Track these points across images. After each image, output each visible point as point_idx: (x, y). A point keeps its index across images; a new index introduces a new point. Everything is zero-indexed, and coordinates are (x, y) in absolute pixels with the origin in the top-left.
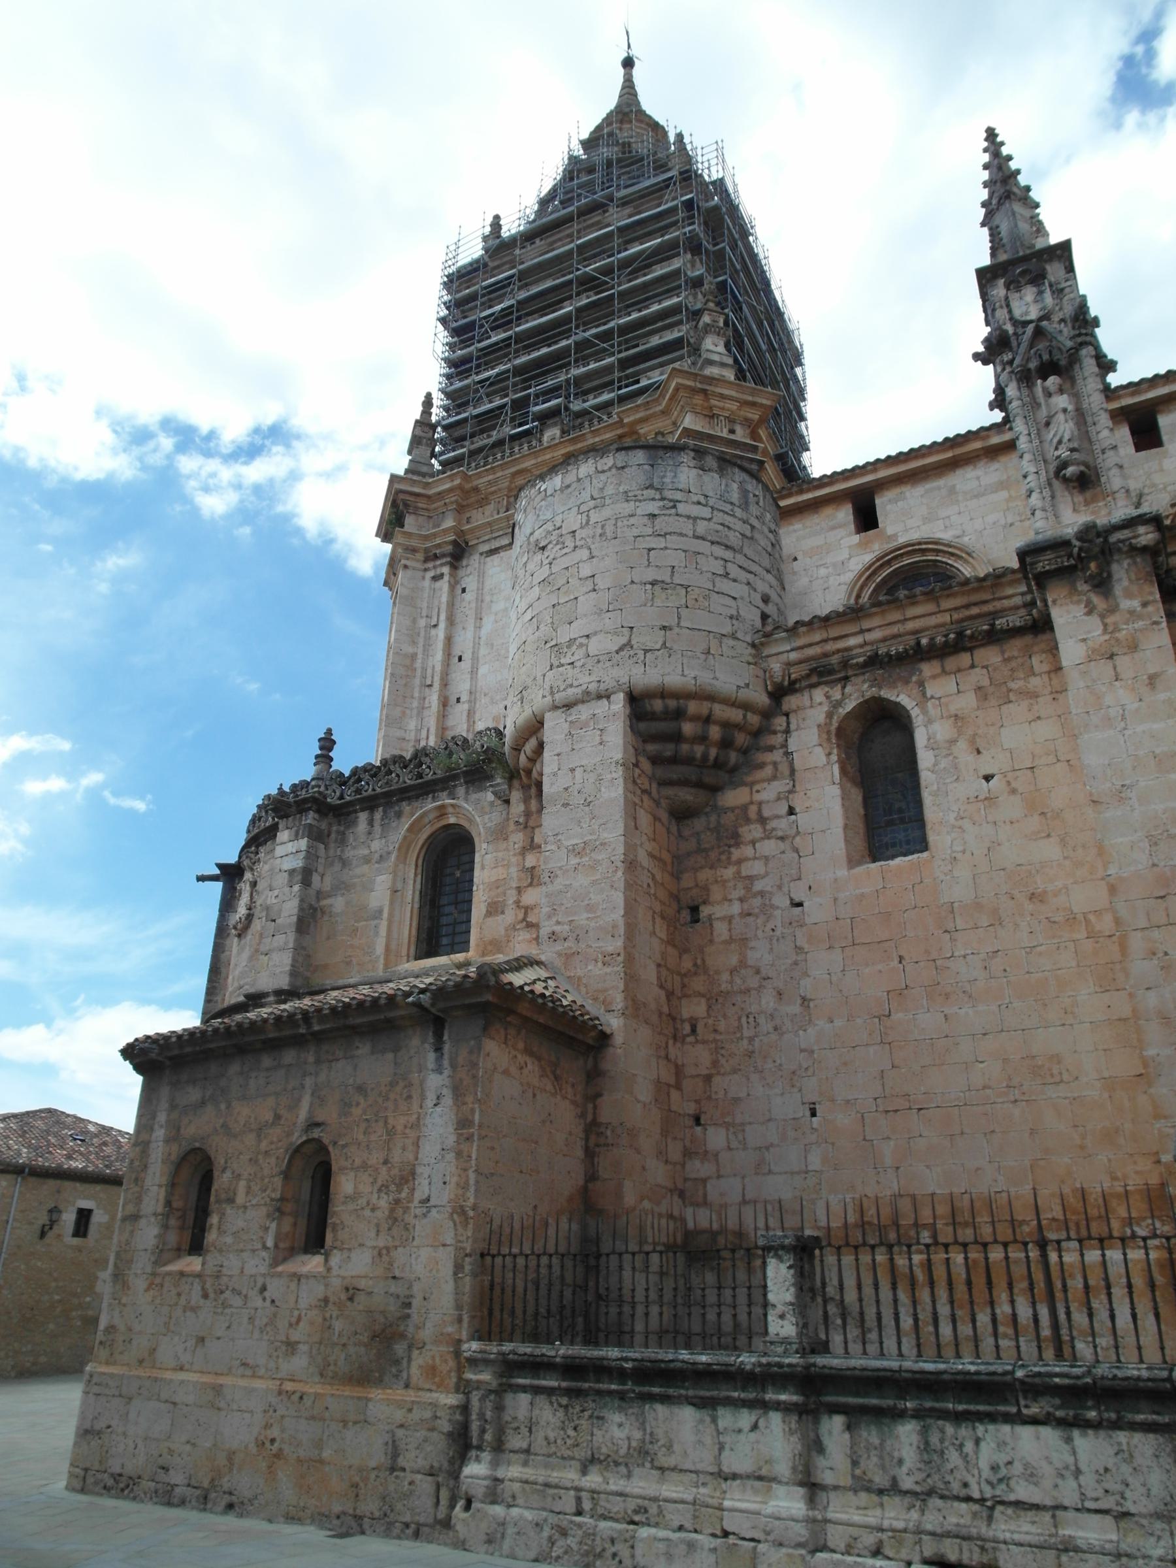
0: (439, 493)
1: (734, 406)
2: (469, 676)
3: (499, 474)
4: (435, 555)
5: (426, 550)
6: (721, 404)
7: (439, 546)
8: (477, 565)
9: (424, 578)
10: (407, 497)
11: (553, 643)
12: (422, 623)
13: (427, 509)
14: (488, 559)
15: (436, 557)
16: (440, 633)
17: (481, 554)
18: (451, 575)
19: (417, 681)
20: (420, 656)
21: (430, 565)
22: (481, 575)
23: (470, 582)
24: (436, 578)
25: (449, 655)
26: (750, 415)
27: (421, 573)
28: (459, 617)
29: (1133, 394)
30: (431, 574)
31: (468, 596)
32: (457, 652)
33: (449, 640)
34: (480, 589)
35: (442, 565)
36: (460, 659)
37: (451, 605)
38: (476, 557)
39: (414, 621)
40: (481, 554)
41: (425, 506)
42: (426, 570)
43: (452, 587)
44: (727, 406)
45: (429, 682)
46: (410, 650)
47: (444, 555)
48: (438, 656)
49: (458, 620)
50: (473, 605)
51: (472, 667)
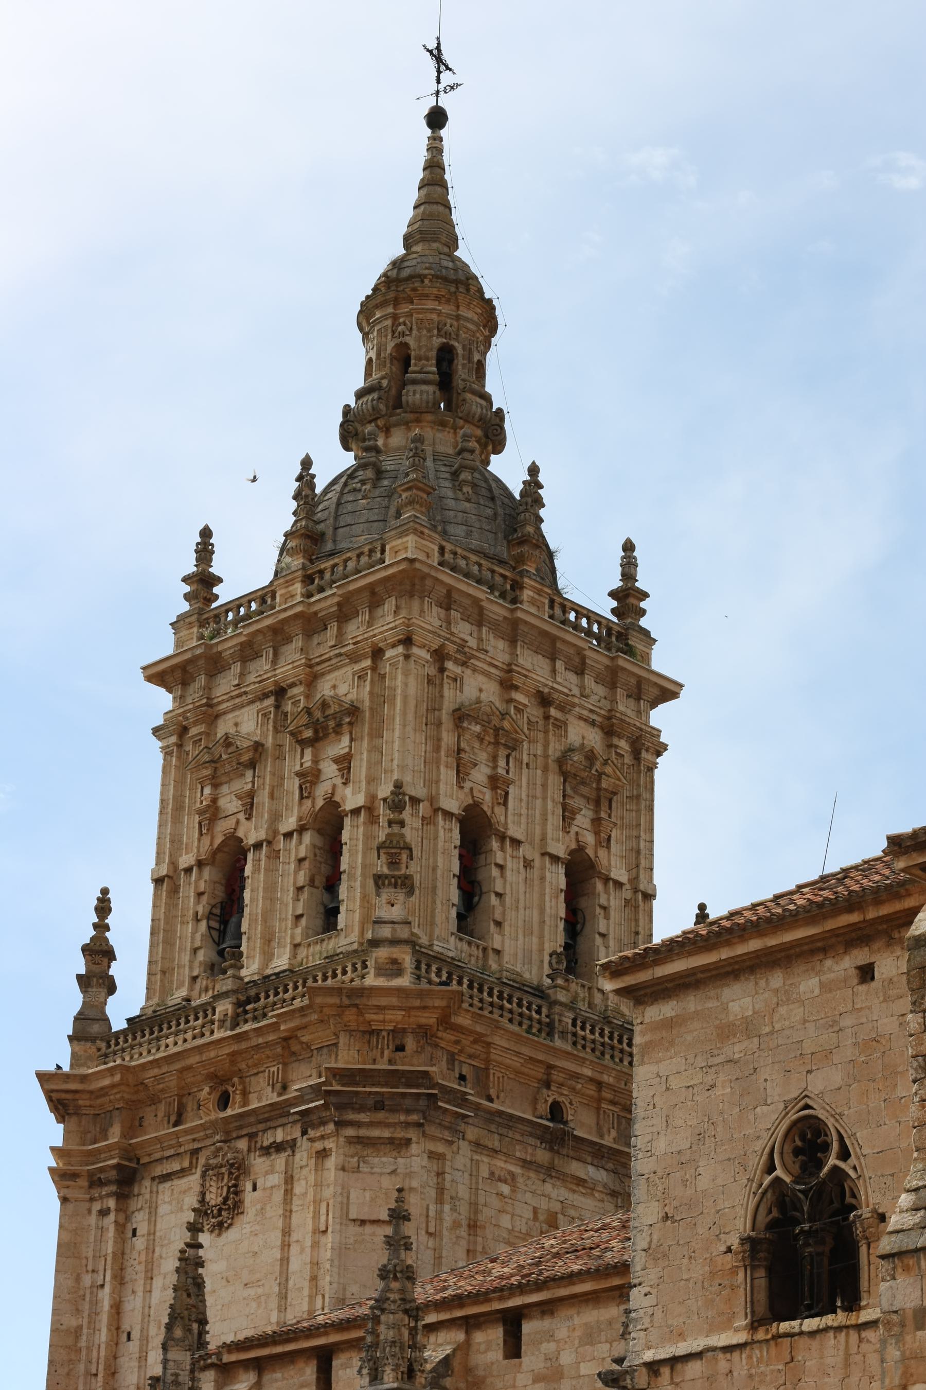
0: (102, 1089)
1: (398, 1015)
2: (136, 1364)
3: (165, 1069)
4: (100, 1179)
5: (91, 1174)
6: (381, 1017)
7: (101, 1170)
8: (147, 1196)
9: (90, 1211)
10: (64, 1096)
11: (251, 1292)
12: (87, 1280)
13: (90, 1106)
14: (161, 1187)
15: (101, 1183)
16: (105, 1297)
17: (153, 1179)
18: (118, 1210)
19: (81, 1367)
20: (85, 1331)
21: (96, 1193)
22: (153, 1211)
23: (140, 1221)
24: (104, 1213)
25: (118, 1329)
26: (423, 1021)
27: (87, 1205)
28: (129, 1274)
29: (501, 1299)
30: (97, 1206)
31: (139, 1243)
32: (126, 1327)
33: (117, 1309)
34: (152, 1233)
35: (108, 1195)
36: (129, 1339)
37: (120, 1255)
38: (147, 1183)
39: (78, 1279)
40: (153, 1179)
41: (88, 1103)
42: (92, 1200)
43: (120, 1227)
44: (388, 1017)
45: (94, 1371)
46: (74, 1323)
47: (108, 1182)
48: (103, 1336)
49: (127, 1278)
50: (143, 1258)
51: (140, 1352)
